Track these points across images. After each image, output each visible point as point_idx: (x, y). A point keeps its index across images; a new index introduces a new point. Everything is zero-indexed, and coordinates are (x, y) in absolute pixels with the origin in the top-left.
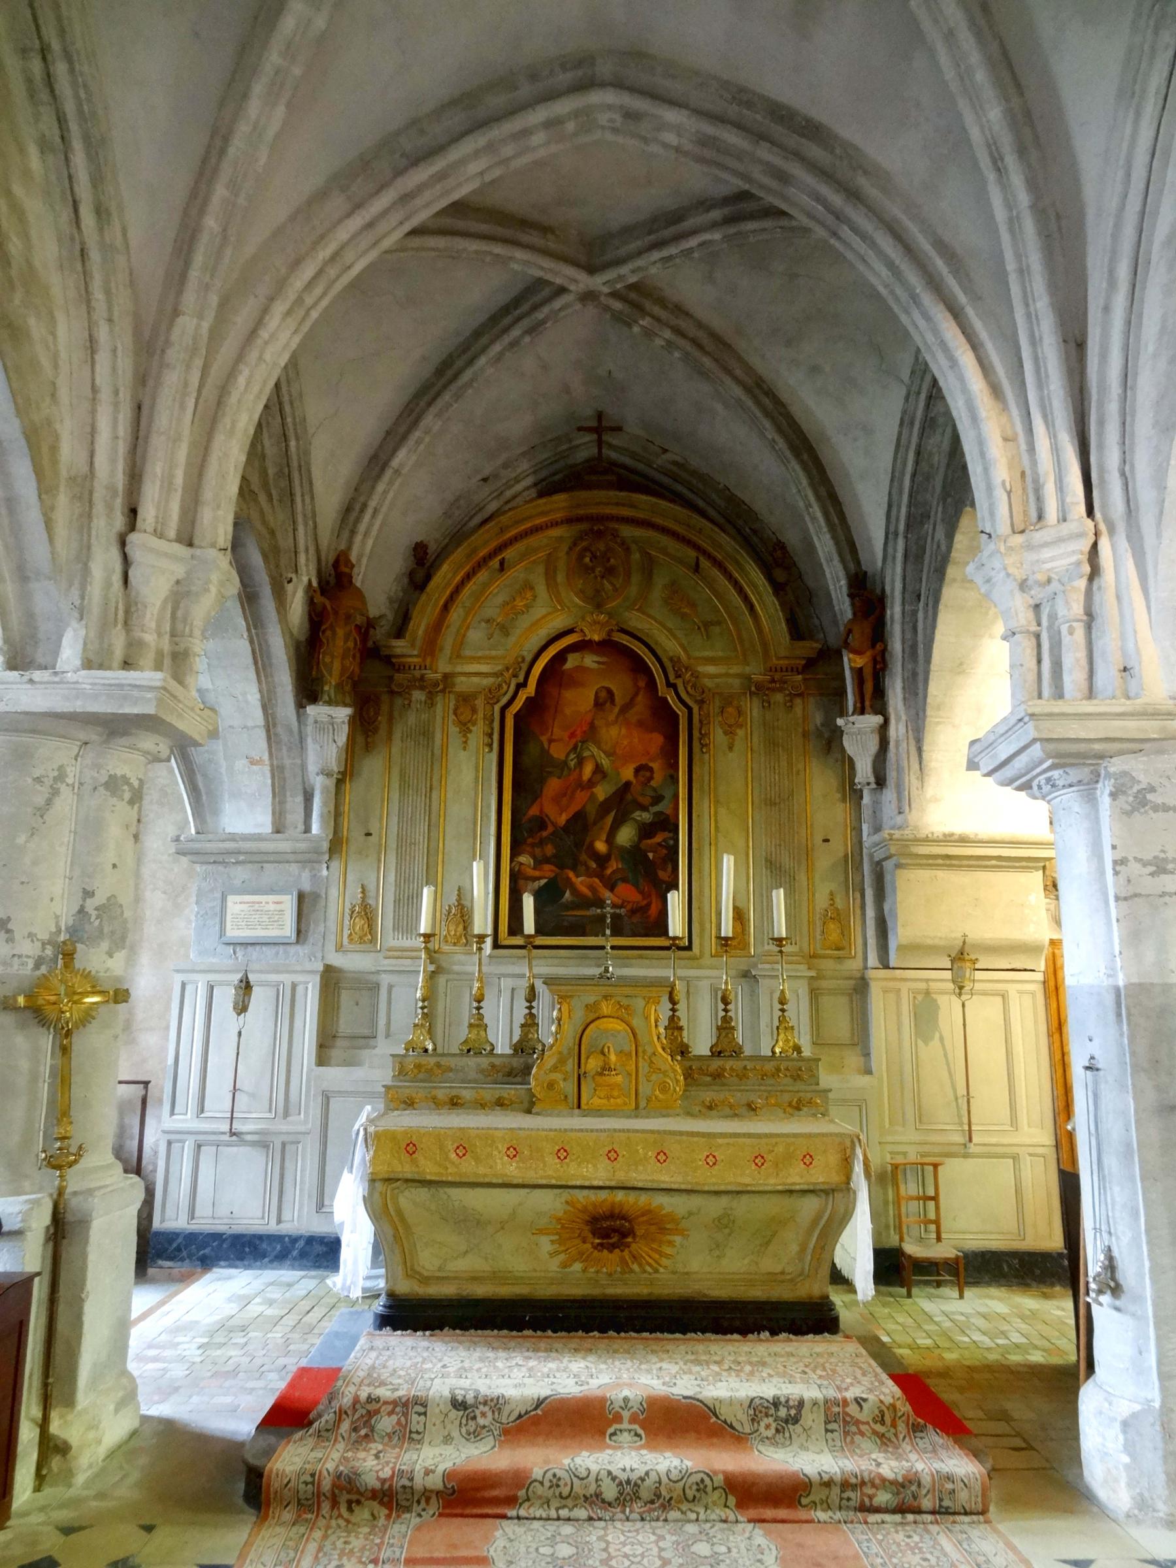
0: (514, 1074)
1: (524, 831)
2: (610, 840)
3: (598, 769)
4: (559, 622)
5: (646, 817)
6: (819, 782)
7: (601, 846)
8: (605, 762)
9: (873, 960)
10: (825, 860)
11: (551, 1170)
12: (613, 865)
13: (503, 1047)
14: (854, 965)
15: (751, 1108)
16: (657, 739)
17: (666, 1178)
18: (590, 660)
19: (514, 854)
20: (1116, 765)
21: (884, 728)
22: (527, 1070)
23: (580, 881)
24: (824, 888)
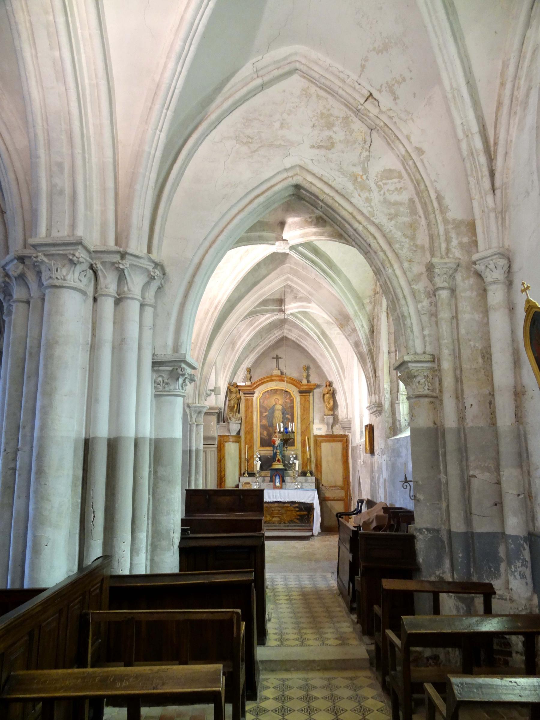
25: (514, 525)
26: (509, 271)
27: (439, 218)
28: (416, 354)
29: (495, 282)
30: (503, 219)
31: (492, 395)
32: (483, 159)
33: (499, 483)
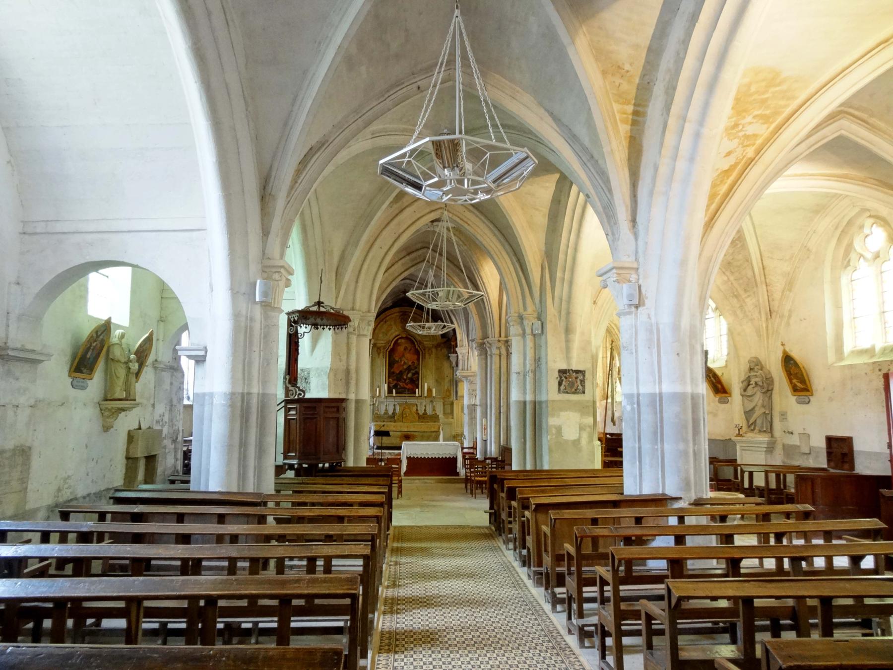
1: (391, 374)
4: (397, 333)
6: (446, 365)
10: (447, 380)
11: (399, 429)
16: (416, 357)
18: (403, 340)
24: (446, 385)
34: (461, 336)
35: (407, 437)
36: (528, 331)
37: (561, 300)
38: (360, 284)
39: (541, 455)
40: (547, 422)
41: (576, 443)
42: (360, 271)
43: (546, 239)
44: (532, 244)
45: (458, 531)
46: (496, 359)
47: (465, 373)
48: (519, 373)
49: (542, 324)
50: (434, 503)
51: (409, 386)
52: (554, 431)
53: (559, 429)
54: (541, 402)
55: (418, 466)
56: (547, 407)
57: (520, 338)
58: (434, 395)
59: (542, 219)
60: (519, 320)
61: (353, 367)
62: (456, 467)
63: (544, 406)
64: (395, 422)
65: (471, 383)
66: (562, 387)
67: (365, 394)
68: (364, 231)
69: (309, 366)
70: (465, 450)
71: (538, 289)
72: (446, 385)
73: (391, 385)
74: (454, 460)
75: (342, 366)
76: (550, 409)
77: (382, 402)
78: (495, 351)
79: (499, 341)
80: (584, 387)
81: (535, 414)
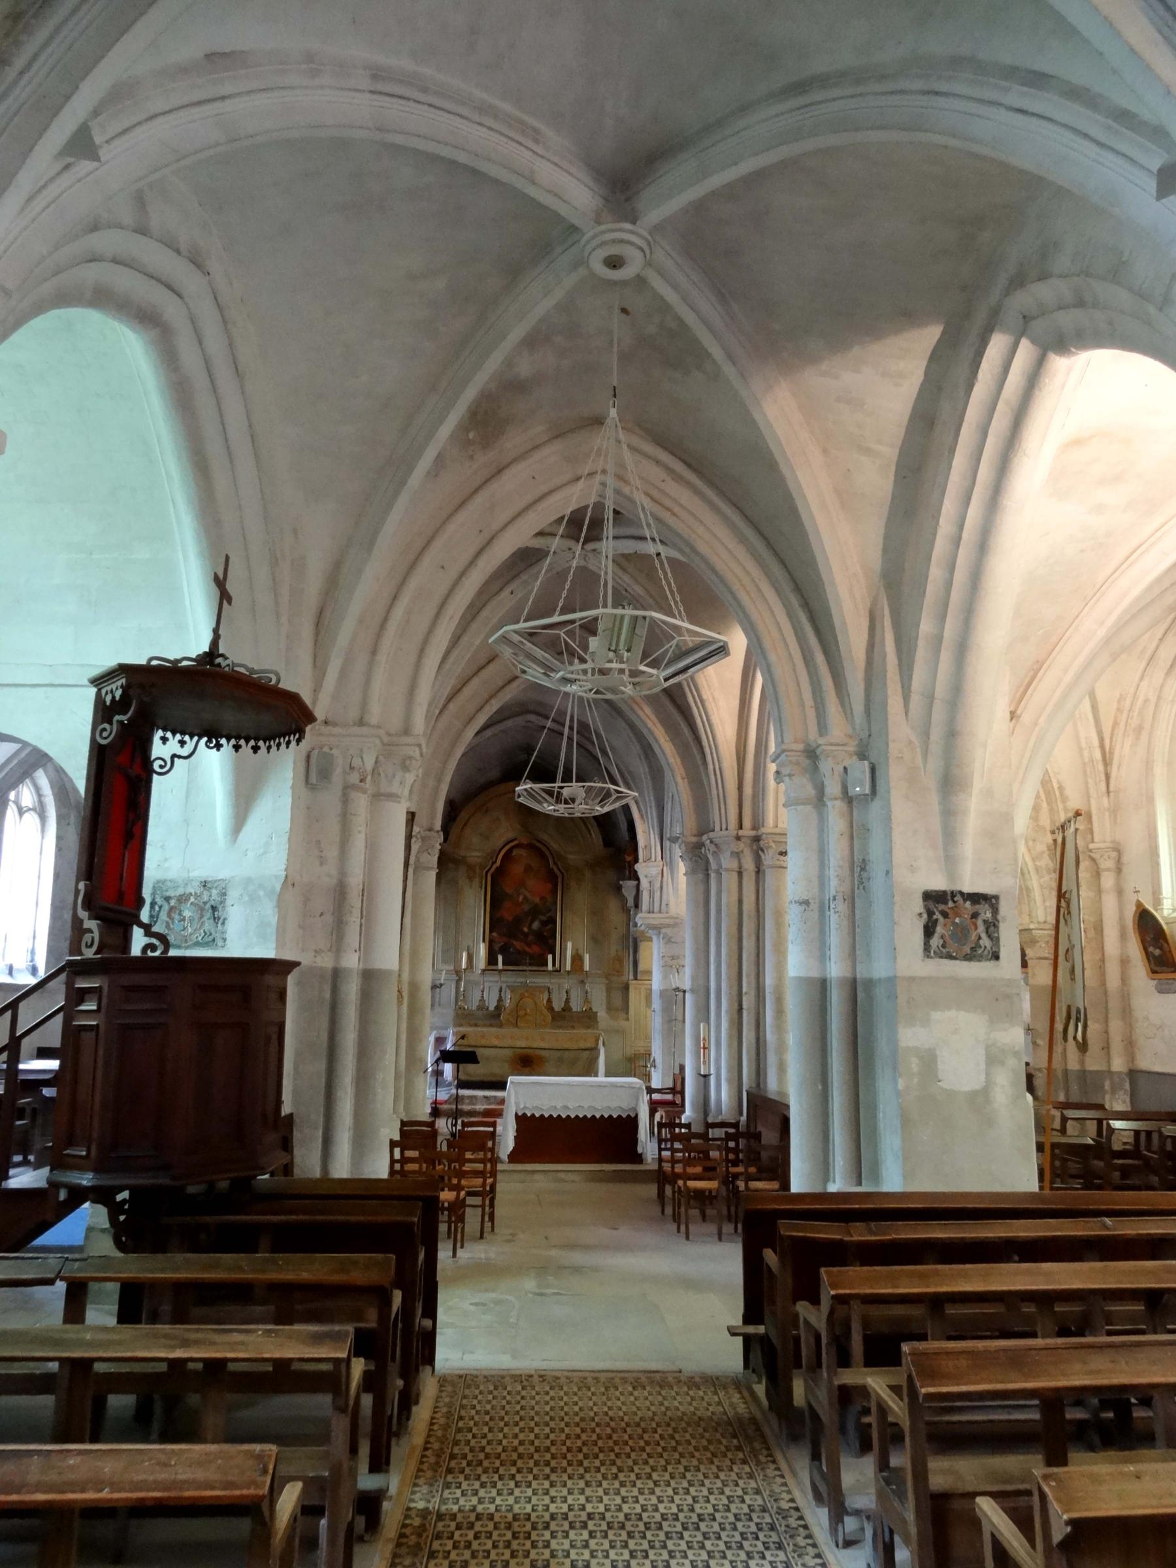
0: (495, 1017)
1: (495, 923)
2: (530, 927)
3: (525, 898)
4: (510, 835)
5: (544, 918)
6: (613, 904)
7: (526, 930)
8: (528, 894)
9: (631, 977)
11: (509, 1042)
12: (530, 938)
13: (492, 1008)
14: (625, 978)
15: (573, 1027)
16: (550, 886)
17: (543, 1045)
19: (491, 932)
20: (663, 931)
21: (638, 886)
22: (499, 1015)
23: (518, 945)
24: (613, 949)
25: (1118, 1064)
26: (1119, 861)
27: (1061, 806)
28: (1039, 923)
29: (1108, 870)
30: (1115, 817)
31: (1103, 960)
32: (1101, 767)
33: (1106, 1032)
34: (646, 836)
35: (527, 1063)
36: (833, 788)
37: (930, 698)
38: (382, 658)
39: (874, 1130)
40: (893, 1041)
41: (980, 1099)
42: (385, 620)
43: (887, 537)
44: (846, 552)
45: (644, 1403)
46: (730, 881)
47: (655, 919)
48: (806, 903)
49: (873, 770)
50: (578, 1258)
51: (535, 949)
52: (914, 1064)
53: (929, 1060)
54: (870, 983)
55: (545, 1138)
56: (893, 996)
57: (808, 809)
58: (587, 967)
59: (876, 480)
60: (806, 762)
61: (356, 879)
62: (635, 1141)
63: (880, 992)
64: (501, 1026)
65: (669, 941)
66: (935, 942)
67: (388, 956)
68: (389, 506)
69: (222, 874)
70: (656, 1096)
71: (860, 675)
72: (613, 949)
73: (496, 947)
74: (629, 1124)
75: (327, 876)
76: (902, 999)
77: (477, 984)
78: (728, 862)
79: (738, 838)
80: (995, 940)
81: (854, 1019)
